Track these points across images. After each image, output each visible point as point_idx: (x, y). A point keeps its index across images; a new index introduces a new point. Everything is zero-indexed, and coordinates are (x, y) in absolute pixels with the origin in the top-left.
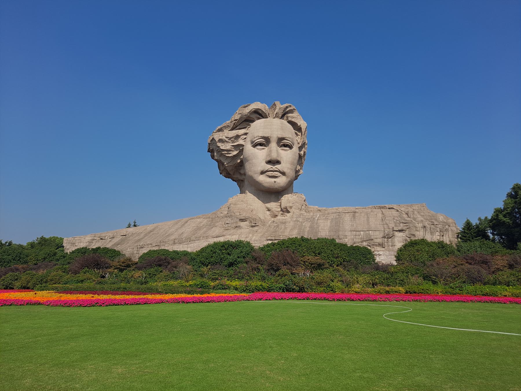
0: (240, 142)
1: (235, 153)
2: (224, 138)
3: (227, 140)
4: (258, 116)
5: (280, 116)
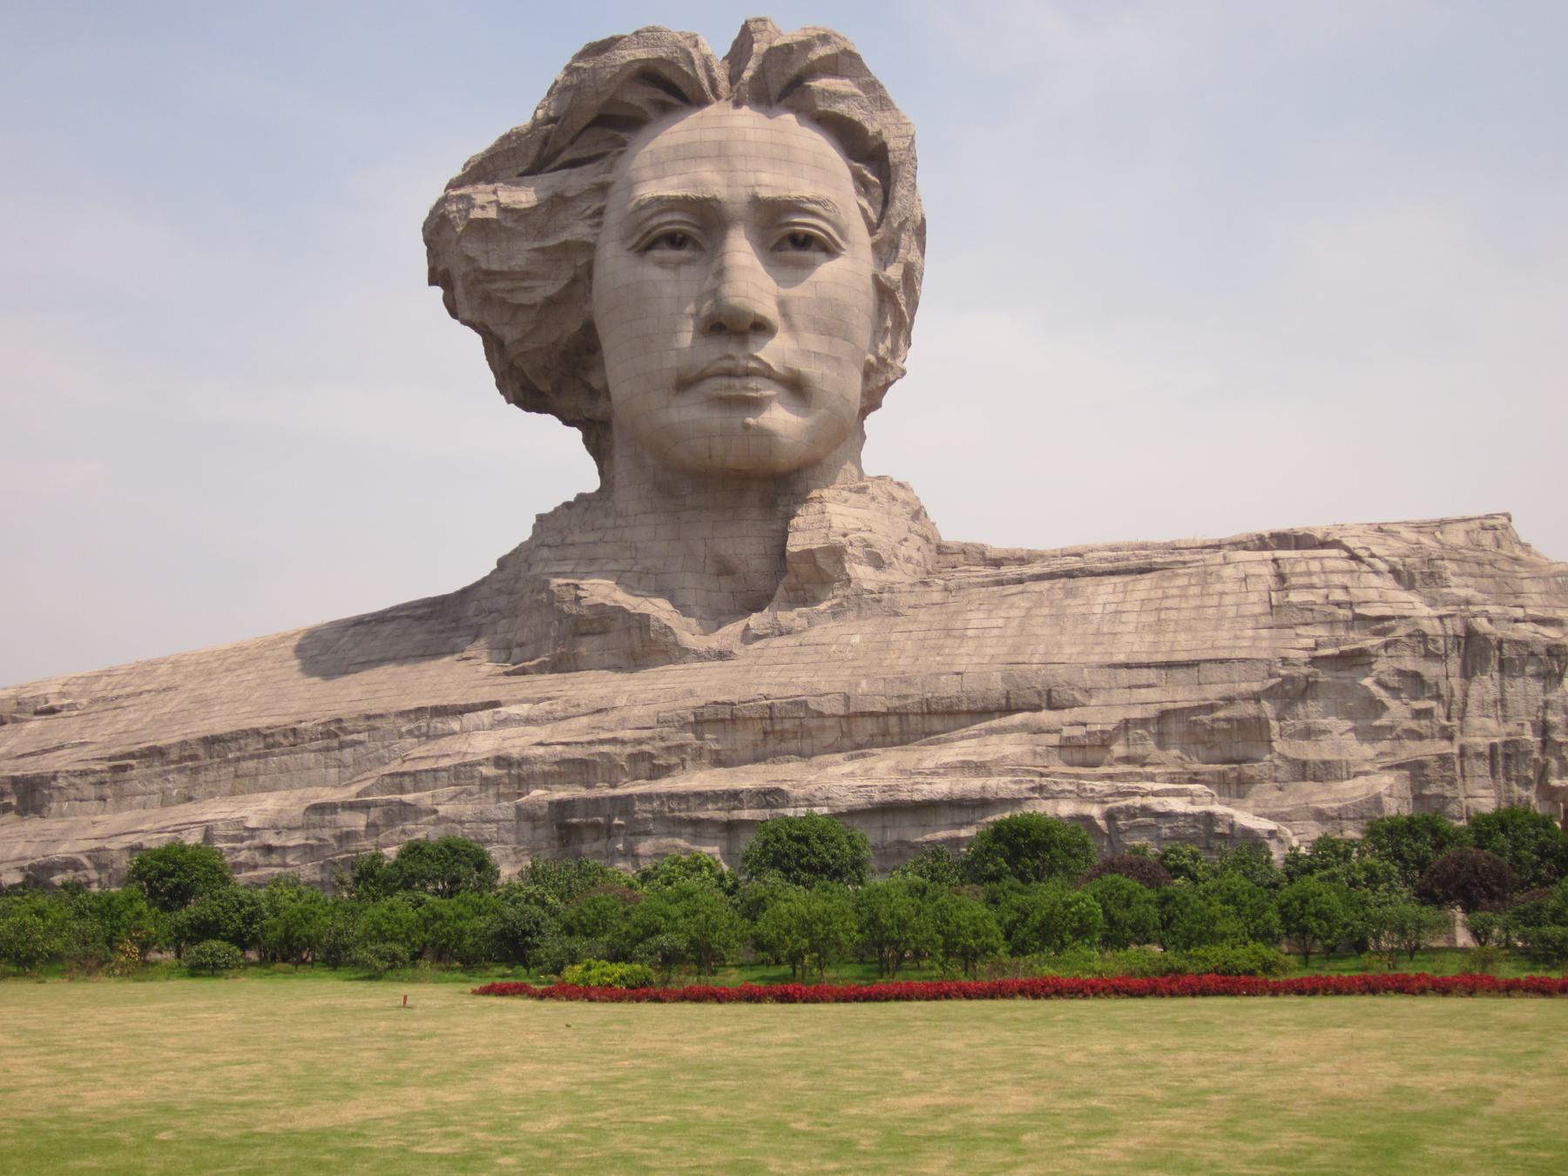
0: (579, 231)
3: (509, 224)
4: (661, 95)
5: (776, 88)
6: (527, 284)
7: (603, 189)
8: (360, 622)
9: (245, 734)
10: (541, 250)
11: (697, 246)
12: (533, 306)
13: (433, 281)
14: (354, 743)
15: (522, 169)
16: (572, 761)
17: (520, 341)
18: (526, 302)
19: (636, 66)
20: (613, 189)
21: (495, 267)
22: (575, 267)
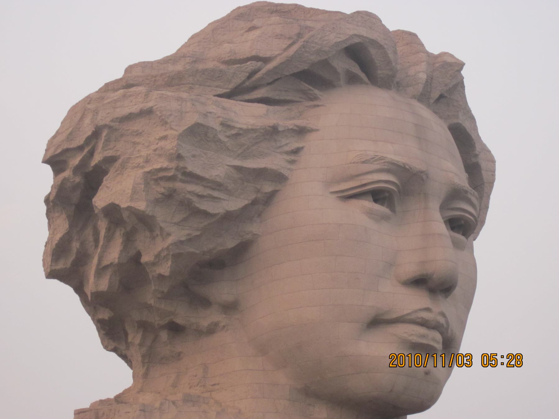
0: (274, 161)
1: (234, 204)
2: (214, 124)
3: (222, 137)
4: (356, 69)
5: (435, 95)
6: (216, 194)
7: (301, 132)
10: (239, 169)
11: (392, 207)
13: (45, 161)
15: (221, 91)
17: (182, 242)
18: (211, 210)
19: (357, 40)
20: (312, 137)
21: (198, 171)
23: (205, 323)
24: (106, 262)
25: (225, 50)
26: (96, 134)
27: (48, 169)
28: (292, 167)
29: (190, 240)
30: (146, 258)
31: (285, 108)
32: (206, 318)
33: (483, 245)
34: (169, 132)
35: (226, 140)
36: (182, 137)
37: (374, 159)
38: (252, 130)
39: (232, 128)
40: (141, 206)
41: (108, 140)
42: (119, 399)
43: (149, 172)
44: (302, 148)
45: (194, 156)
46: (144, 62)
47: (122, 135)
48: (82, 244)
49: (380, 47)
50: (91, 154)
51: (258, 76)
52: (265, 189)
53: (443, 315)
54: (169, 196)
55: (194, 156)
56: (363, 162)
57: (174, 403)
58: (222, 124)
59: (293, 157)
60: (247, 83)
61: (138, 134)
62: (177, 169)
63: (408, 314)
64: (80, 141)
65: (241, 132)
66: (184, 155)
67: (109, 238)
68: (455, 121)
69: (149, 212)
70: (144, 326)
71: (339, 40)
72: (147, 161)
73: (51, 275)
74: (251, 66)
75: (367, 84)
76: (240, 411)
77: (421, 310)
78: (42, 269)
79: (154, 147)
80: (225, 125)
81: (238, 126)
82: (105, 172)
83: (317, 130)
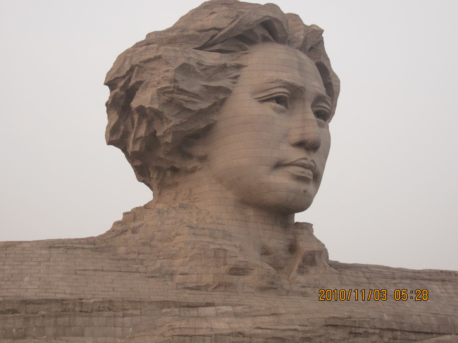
0: (225, 83)
1: (204, 105)
2: (193, 63)
5: (308, 47)
6: (195, 100)
7: (239, 67)
8: (52, 245)
9: (48, 301)
10: (206, 87)
11: (286, 106)
12: (194, 111)
13: (106, 84)
14: (132, 315)
16: (277, 338)
17: (177, 125)
19: (267, 19)
20: (245, 69)
21: (185, 88)
22: (217, 98)
23: (190, 167)
24: (138, 136)
25: (198, 25)
26: (132, 69)
27: (107, 88)
28: (234, 85)
29: (182, 124)
30: (159, 134)
31: (230, 54)
32: (190, 164)
33: (334, 125)
34: (170, 68)
35: (199, 72)
36: (176, 70)
37: (277, 81)
38: (213, 66)
39: (203, 65)
40: (156, 106)
41: (138, 73)
42: (146, 207)
43: (159, 89)
44: (239, 75)
45: (183, 80)
46: (156, 32)
47: (145, 70)
48: (125, 127)
49: (279, 22)
50: (129, 80)
51: (216, 38)
52: (220, 97)
53: (313, 161)
54: (170, 102)
55: (183, 80)
56: (271, 83)
57: (174, 208)
58: (198, 63)
59: (234, 80)
60: (210, 42)
61: (154, 69)
62: (174, 87)
63: (295, 161)
64: (123, 73)
65: (207, 67)
66: (177, 79)
67: (140, 124)
68: (319, 61)
69: (160, 110)
70: (158, 169)
71: (258, 19)
72: (159, 83)
73: (109, 143)
74: (212, 33)
75: (273, 42)
76: (208, 212)
77: (302, 159)
78: (105, 140)
79: (162, 76)
80: (199, 64)
81: (206, 64)
82: (137, 89)
83: (247, 66)
